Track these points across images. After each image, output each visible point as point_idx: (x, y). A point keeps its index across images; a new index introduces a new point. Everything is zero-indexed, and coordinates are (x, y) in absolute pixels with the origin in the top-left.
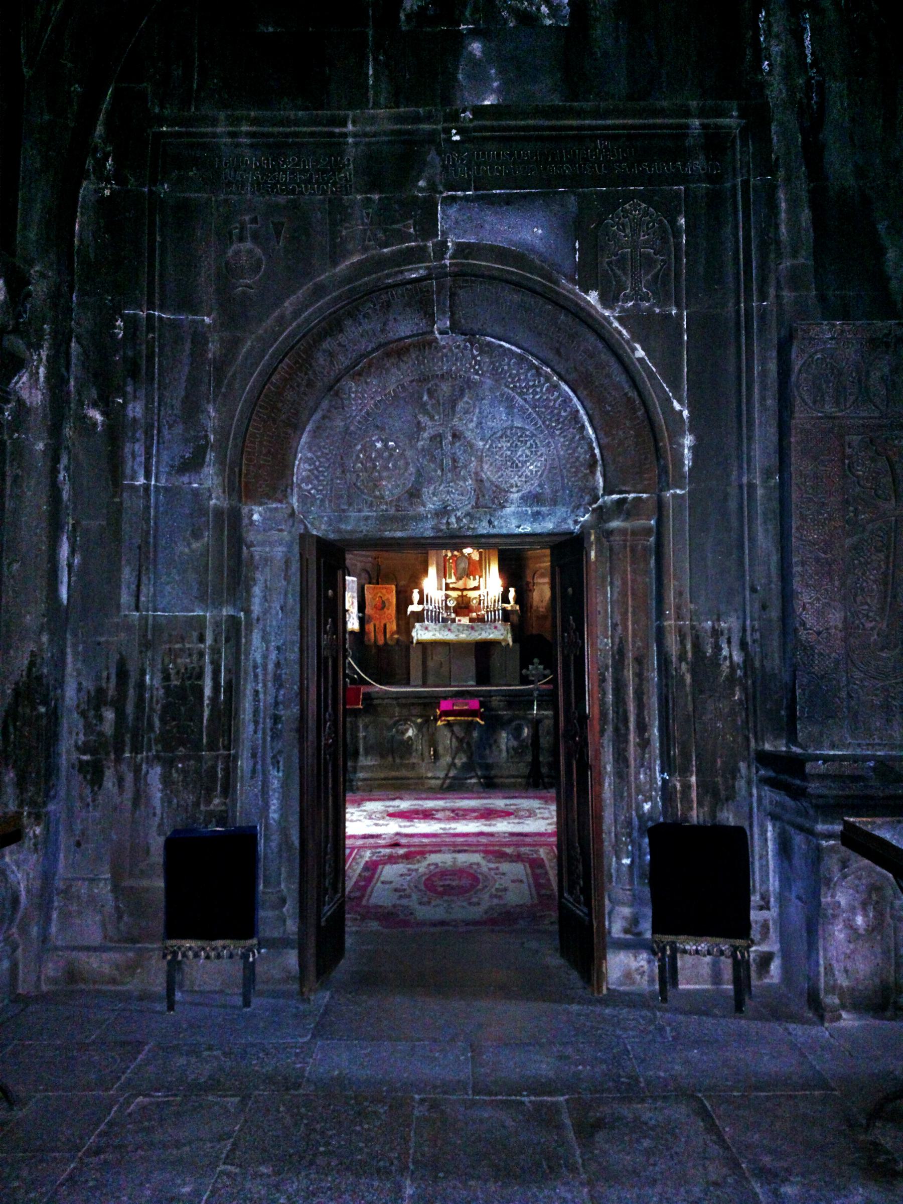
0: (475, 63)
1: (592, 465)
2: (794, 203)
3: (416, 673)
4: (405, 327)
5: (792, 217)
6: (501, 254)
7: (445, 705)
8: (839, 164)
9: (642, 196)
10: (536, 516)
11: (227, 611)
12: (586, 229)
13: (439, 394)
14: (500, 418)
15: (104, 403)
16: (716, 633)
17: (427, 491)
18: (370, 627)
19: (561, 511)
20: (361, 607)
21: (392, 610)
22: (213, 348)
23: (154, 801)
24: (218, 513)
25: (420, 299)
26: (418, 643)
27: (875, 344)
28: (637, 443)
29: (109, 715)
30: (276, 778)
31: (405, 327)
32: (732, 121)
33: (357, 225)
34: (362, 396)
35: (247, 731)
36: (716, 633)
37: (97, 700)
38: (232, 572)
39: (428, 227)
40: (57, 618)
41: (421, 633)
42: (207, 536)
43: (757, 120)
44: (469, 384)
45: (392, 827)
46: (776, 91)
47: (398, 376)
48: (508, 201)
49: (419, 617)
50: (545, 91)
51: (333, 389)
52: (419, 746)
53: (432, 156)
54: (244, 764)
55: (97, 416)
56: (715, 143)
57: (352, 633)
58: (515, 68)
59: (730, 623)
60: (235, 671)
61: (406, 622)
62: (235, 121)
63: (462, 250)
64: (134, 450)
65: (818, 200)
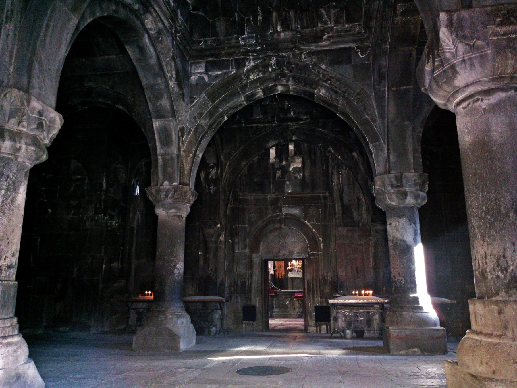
0: (288, 185)
1: (308, 248)
2: (338, 207)
3: (290, 285)
4: (277, 226)
5: (338, 208)
6: (291, 215)
7: (296, 295)
8: (346, 200)
9: (314, 206)
10: (299, 256)
11: (250, 272)
12: (305, 211)
13: (284, 236)
14: (293, 240)
15: (231, 239)
16: (327, 275)
17: (281, 252)
18: (277, 273)
19: (303, 255)
20: (274, 267)
21: (283, 268)
22: (248, 230)
23: (239, 302)
24: (249, 256)
25: (280, 221)
26: (290, 278)
27: (349, 230)
28: (314, 244)
29: (232, 288)
30: (258, 299)
31: (277, 226)
32: (327, 194)
33: (270, 211)
34: (271, 236)
35: (253, 291)
36: (327, 275)
37: (230, 286)
38: (250, 265)
39: (280, 211)
40: (225, 273)
41: (291, 275)
42: (247, 260)
43: (331, 195)
44: (288, 234)
45: (281, 322)
46: (335, 188)
47: (277, 233)
48: (293, 207)
49: (290, 270)
50: (298, 189)
51: (266, 235)
52: (289, 306)
53: (281, 200)
54: (253, 296)
55: (230, 241)
56: (325, 198)
57: (272, 275)
58: (293, 185)
59: (329, 274)
60: (251, 281)
61: (287, 271)
62: (251, 196)
63: (286, 214)
64: (236, 247)
65: (343, 205)
